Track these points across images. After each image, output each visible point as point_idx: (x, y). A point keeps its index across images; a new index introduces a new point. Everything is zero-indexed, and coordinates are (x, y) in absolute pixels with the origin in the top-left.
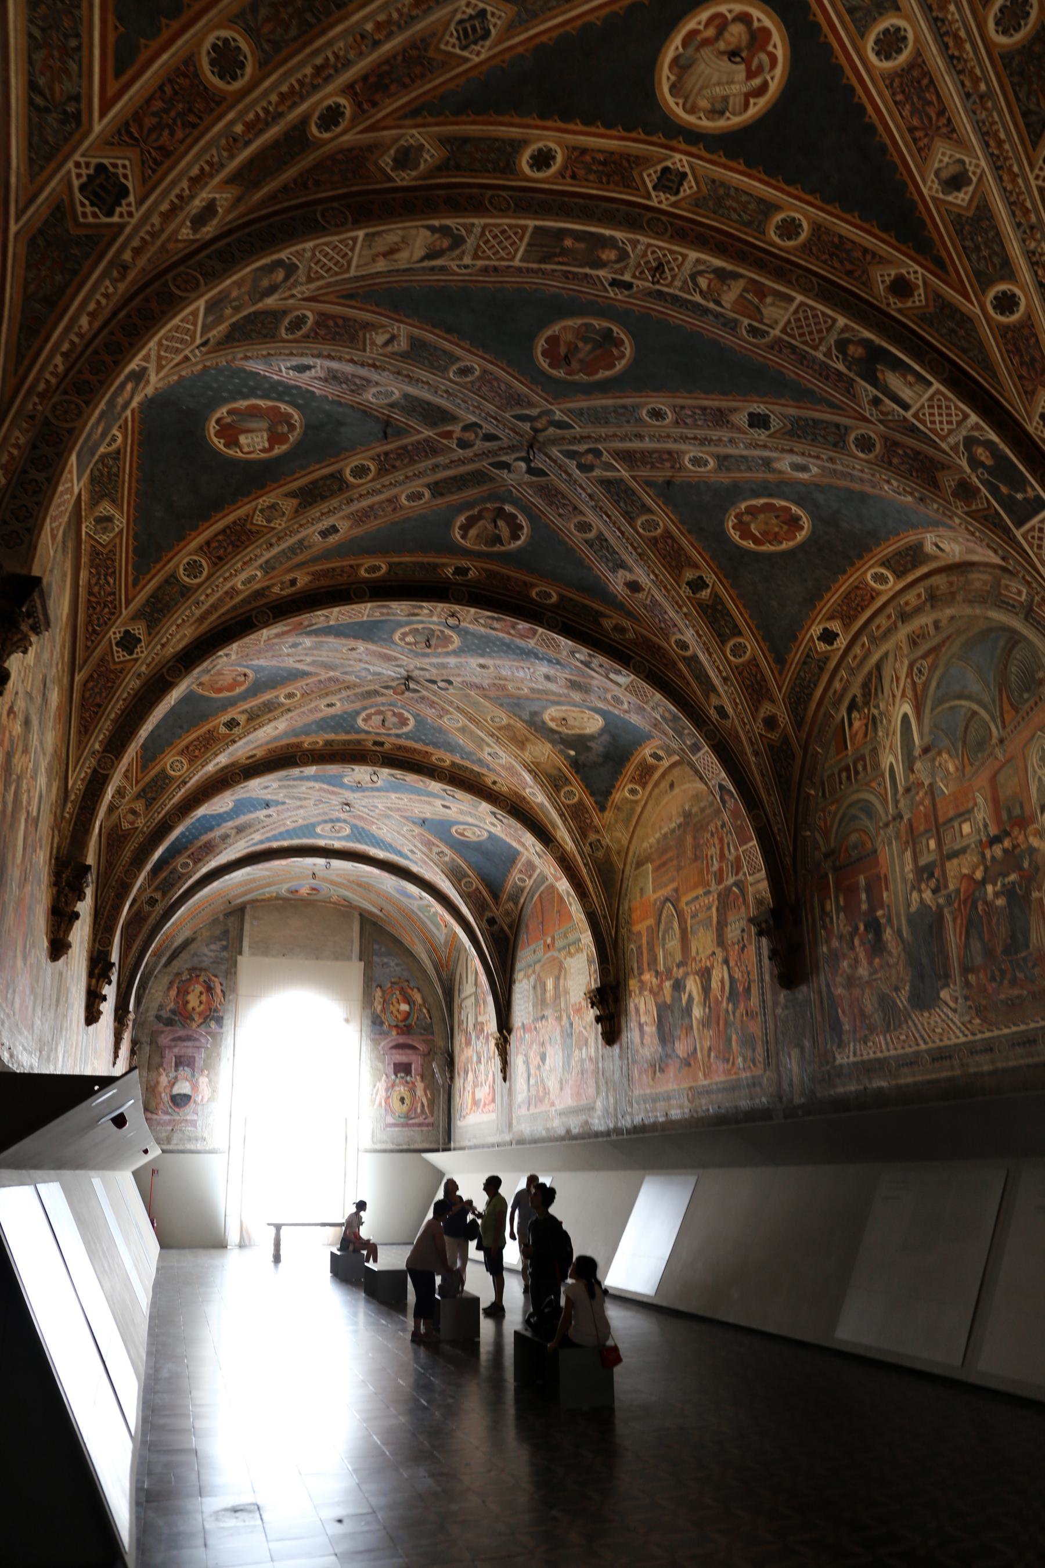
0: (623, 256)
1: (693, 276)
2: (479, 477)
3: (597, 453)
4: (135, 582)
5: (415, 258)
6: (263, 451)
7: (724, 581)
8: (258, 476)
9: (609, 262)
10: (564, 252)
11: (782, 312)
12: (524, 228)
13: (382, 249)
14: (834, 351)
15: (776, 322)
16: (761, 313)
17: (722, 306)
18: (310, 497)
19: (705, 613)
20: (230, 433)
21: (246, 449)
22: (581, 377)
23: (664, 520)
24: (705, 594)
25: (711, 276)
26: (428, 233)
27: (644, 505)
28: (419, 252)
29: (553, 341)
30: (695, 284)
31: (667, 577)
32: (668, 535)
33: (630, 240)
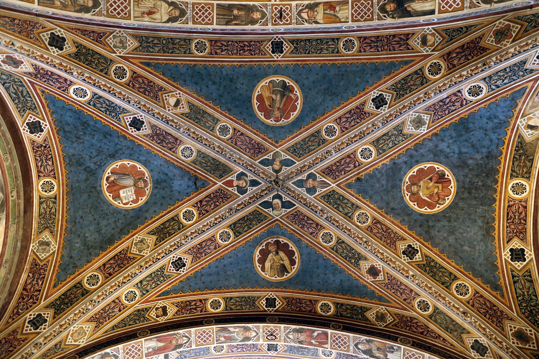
0: (264, 15)
1: (299, 14)
2: (256, 217)
3: (311, 176)
4: (55, 286)
5: (164, 20)
6: (134, 202)
7: (426, 244)
8: (133, 220)
9: (258, 19)
10: (236, 18)
11: (347, 11)
12: (213, 4)
13: (146, 10)
14: (381, 15)
15: (348, 18)
16: (338, 17)
17: (318, 23)
18: (163, 233)
19: (426, 271)
20: (115, 188)
21: (124, 202)
22: (283, 122)
23: (368, 211)
24: (418, 257)
25: (307, 10)
26: (167, 5)
27: (353, 204)
28: (166, 18)
29: (260, 98)
30: (302, 18)
31: (388, 253)
32: (376, 222)
33: (263, 5)
